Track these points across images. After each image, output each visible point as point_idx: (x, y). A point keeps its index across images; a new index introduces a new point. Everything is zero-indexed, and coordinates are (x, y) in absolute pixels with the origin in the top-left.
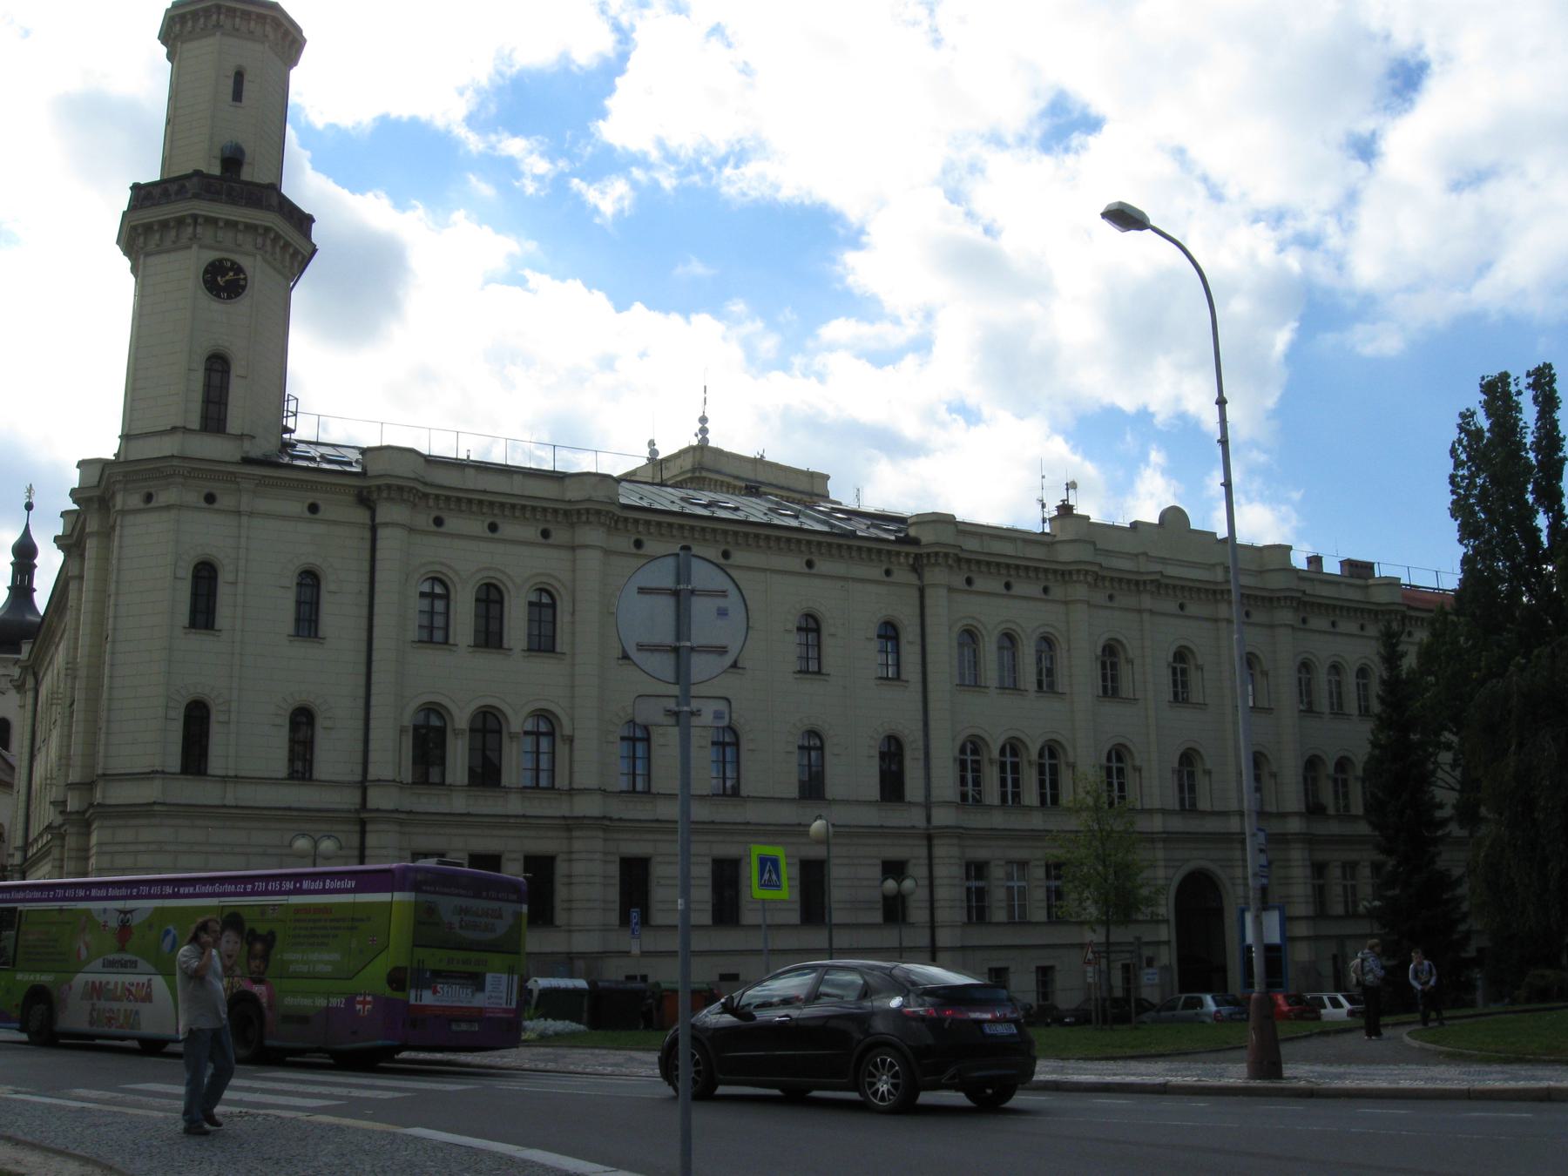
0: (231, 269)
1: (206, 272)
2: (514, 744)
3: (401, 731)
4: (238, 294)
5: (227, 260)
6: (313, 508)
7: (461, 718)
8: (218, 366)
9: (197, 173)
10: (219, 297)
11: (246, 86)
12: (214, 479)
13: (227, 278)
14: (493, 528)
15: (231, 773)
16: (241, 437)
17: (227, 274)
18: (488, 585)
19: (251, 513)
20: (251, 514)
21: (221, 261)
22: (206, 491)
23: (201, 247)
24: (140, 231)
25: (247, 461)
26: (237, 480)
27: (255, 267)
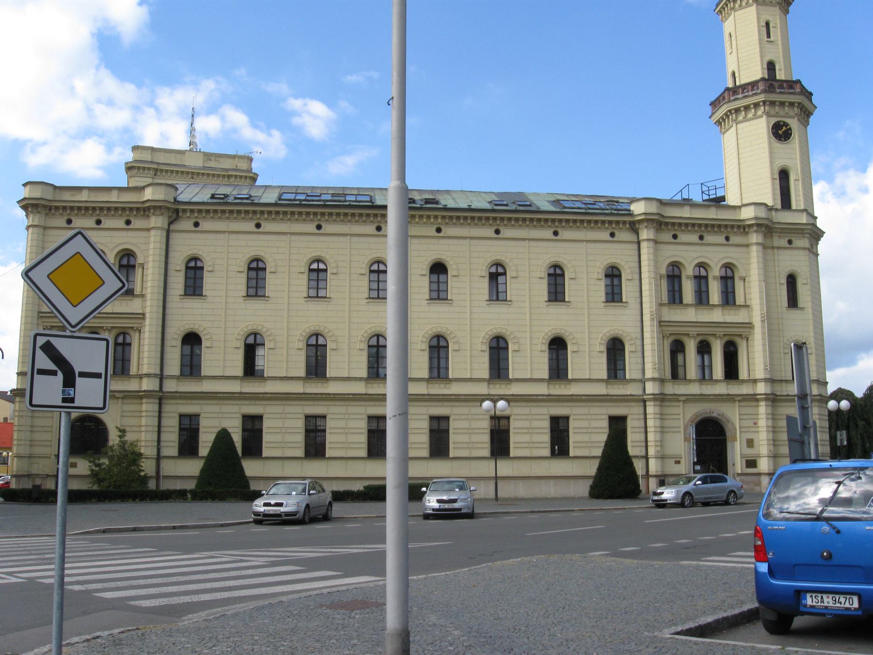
1: (773, 128)
8: (784, 175)
9: (763, 79)
11: (771, 29)
13: (783, 130)
21: (778, 122)
22: (788, 238)
24: (733, 111)
27: (794, 124)
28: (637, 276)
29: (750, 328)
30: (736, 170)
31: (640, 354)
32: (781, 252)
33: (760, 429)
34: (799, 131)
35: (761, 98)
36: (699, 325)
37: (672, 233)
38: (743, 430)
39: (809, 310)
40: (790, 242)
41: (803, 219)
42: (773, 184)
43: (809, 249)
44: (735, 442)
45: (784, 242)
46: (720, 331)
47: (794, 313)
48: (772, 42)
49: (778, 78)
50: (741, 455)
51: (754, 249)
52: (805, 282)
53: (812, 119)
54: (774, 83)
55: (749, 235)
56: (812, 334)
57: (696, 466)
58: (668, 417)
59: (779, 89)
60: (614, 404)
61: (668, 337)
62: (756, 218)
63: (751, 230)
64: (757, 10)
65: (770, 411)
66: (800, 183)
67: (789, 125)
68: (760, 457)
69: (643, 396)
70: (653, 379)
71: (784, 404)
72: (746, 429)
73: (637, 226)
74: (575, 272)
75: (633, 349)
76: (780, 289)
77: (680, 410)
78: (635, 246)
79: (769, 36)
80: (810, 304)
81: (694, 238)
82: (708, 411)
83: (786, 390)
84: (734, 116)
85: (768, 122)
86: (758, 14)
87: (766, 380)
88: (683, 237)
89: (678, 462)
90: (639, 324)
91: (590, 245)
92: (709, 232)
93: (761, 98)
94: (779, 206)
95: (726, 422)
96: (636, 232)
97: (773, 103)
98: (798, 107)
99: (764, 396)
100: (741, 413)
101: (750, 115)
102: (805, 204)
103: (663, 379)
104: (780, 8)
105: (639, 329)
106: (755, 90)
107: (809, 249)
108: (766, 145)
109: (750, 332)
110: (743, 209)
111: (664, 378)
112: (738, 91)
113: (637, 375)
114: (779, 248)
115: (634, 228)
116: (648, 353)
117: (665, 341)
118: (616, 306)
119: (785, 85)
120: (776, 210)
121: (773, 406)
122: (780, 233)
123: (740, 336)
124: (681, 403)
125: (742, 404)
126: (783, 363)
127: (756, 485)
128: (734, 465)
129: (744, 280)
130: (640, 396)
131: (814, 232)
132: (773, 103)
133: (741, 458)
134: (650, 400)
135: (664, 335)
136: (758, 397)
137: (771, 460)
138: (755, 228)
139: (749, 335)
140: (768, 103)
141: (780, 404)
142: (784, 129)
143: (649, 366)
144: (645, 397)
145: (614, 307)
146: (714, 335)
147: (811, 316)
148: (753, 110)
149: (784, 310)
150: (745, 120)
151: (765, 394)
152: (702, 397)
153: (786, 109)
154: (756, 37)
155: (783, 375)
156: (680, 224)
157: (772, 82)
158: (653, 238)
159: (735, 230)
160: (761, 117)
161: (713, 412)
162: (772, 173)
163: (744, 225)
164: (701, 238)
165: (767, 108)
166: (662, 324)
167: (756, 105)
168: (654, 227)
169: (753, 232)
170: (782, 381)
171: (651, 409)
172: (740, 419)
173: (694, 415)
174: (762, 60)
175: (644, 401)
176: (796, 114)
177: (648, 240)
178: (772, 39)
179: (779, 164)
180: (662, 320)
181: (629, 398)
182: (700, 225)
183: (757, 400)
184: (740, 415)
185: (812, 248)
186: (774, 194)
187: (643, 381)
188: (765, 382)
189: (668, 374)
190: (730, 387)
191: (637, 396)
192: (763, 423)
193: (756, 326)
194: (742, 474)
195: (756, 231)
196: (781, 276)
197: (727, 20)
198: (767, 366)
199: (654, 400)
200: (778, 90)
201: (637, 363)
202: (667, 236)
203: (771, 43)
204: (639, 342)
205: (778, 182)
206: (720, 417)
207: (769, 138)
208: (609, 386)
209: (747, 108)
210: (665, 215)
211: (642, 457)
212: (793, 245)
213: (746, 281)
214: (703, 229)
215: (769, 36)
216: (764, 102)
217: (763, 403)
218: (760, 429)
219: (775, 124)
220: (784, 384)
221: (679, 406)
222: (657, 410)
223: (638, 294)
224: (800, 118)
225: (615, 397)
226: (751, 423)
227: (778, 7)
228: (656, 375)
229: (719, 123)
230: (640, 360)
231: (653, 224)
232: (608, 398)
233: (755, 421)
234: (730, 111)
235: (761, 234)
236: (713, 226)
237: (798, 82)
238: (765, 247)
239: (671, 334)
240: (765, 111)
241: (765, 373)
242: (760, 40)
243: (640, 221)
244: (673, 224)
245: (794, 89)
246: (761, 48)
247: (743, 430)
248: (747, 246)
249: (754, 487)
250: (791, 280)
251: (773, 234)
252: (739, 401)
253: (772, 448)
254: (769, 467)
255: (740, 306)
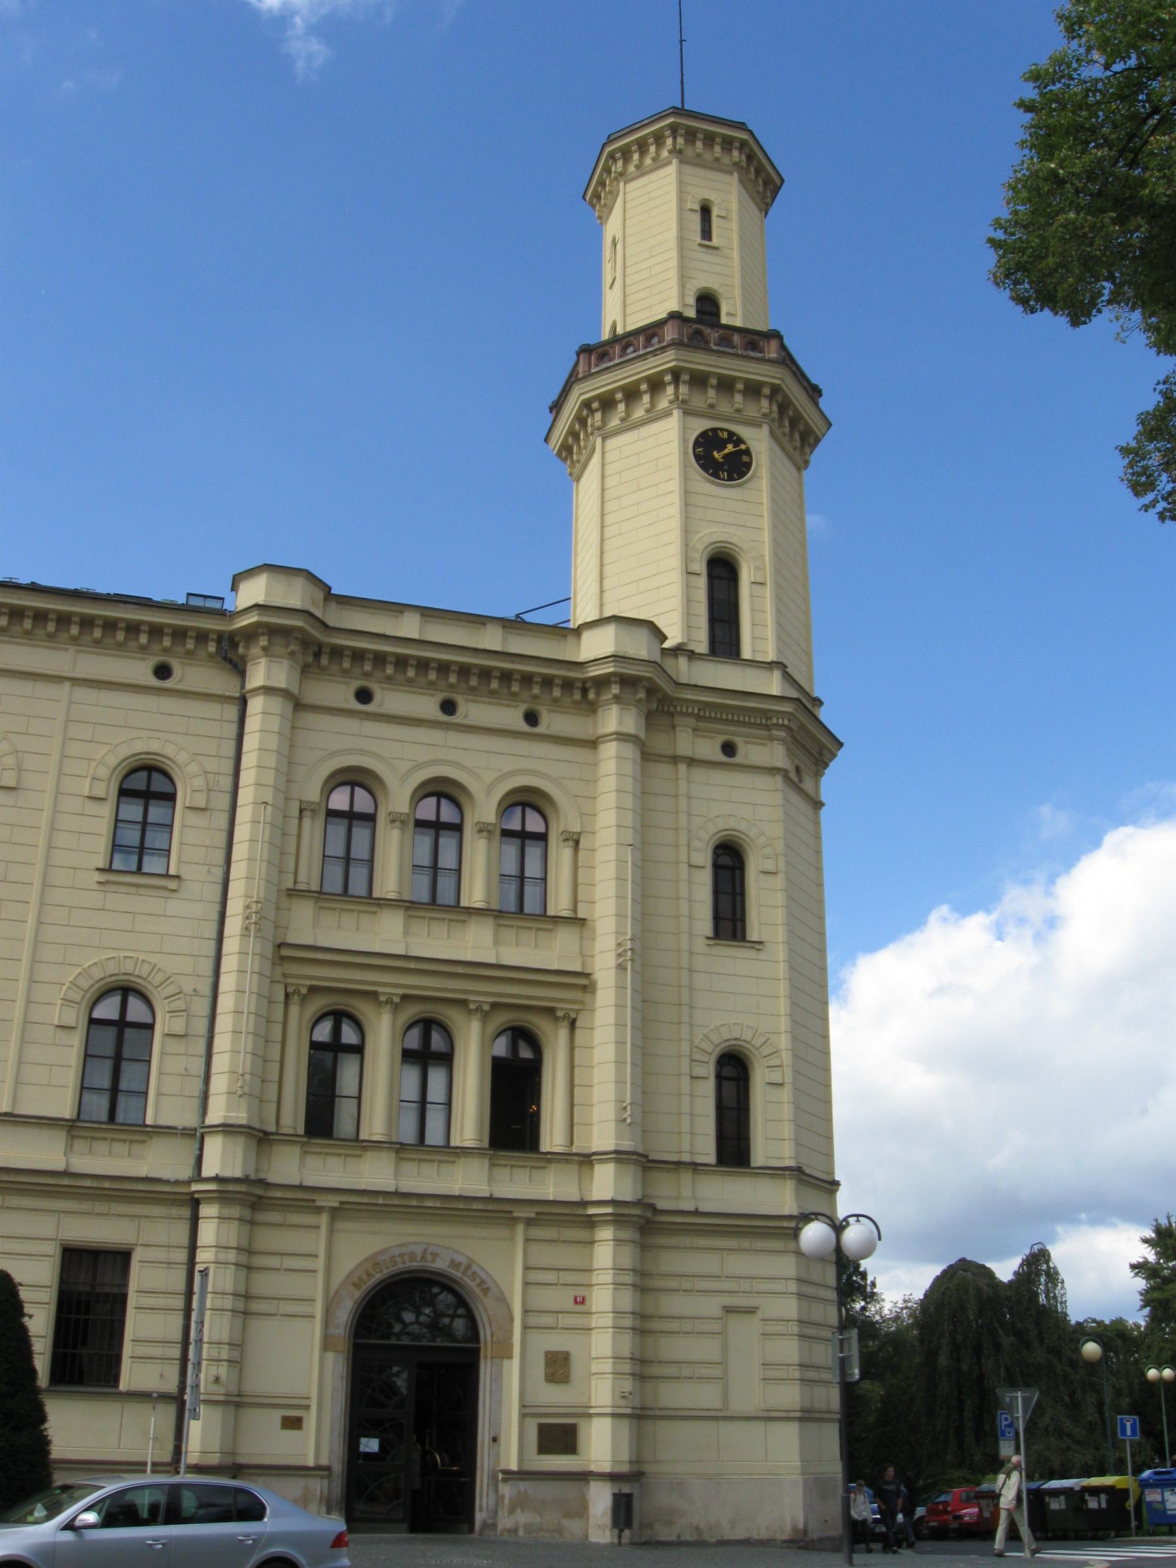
0: (729, 441)
1: (697, 444)
4: (742, 475)
5: (722, 430)
9: (675, 316)
10: (718, 477)
11: (715, 221)
13: (726, 451)
17: (726, 448)
21: (714, 430)
24: (595, 405)
28: (224, 801)
29: (584, 988)
30: (595, 562)
31: (201, 1048)
32: (699, 774)
33: (595, 1321)
34: (772, 462)
35: (666, 361)
36: (412, 965)
37: (356, 684)
38: (534, 1320)
39: (779, 952)
40: (729, 749)
41: (774, 685)
42: (688, 588)
43: (784, 772)
44: (506, 1362)
45: (710, 749)
46: (482, 992)
47: (730, 957)
48: (716, 248)
49: (724, 320)
50: (523, 1406)
51: (609, 750)
52: (769, 865)
53: (817, 457)
54: (707, 331)
55: (600, 711)
56: (784, 1024)
57: (363, 1440)
58: (273, 1262)
59: (718, 345)
60: (86, 1206)
61: (304, 999)
62: (616, 657)
63: (606, 696)
64: (680, 173)
65: (627, 1262)
66: (768, 591)
67: (743, 442)
68: (590, 1416)
69: (189, 1182)
70: (227, 1129)
71: (687, 1241)
72: (547, 1320)
73: (241, 650)
74: (20, 769)
75: (178, 1026)
76: (690, 882)
77: (318, 1242)
78: (232, 712)
79: (707, 233)
80: (780, 934)
81: (427, 705)
82: (418, 1250)
83: (694, 1197)
84: (598, 416)
85: (684, 429)
86: (681, 182)
87: (619, 1156)
88: (388, 700)
89: (293, 1424)
90: (210, 948)
91: (81, 693)
92: (472, 690)
93: (666, 361)
94: (702, 647)
95: (477, 1290)
96: (239, 669)
97: (699, 380)
98: (771, 398)
99: (609, 1210)
100: (532, 1262)
101: (639, 413)
102: (779, 651)
103: (266, 1133)
104: (741, 181)
105: (207, 967)
106: (652, 345)
107: (784, 772)
108: (675, 485)
109: (582, 1002)
110: (587, 636)
111: (272, 1129)
112: (611, 351)
113: (186, 1118)
114: (692, 762)
115: (234, 657)
116: (222, 1042)
117: (294, 1010)
118: (138, 886)
119: (736, 338)
120: (692, 655)
121: (643, 1247)
122: (698, 718)
123: (550, 1012)
124: (324, 1219)
125: (537, 1232)
126: (686, 1108)
127: (569, 1515)
128: (495, 1440)
129: (577, 842)
130: (177, 1183)
131: (802, 727)
132: (699, 380)
133: (523, 1416)
134: (211, 1197)
135: (290, 990)
136: (592, 1211)
137: (625, 1427)
138: (615, 689)
139: (578, 1011)
140: (685, 377)
141: (673, 1241)
142: (730, 448)
143: (219, 1084)
144: (195, 1187)
145: (133, 890)
146: (464, 1003)
147: (782, 970)
148: (646, 398)
149: (700, 944)
150: (628, 426)
151: (613, 1202)
152: (395, 1201)
153: (738, 398)
154: (672, 234)
155: (686, 1146)
156: (380, 659)
157: (702, 327)
158: (283, 685)
159: (557, 692)
160: (667, 414)
161: (435, 1255)
162: (687, 559)
163: (584, 681)
164: (448, 707)
165: (684, 389)
166: (285, 952)
167: (655, 385)
168: (292, 654)
169: (608, 702)
170: (679, 1163)
171: (208, 1232)
172: (526, 1284)
173: (366, 1261)
174: (682, 286)
175: (195, 1203)
176: (764, 415)
177: (267, 690)
178: (715, 241)
179: (710, 534)
180: (291, 939)
181: (140, 1187)
182: (444, 668)
183: (591, 1223)
184: (527, 1268)
185: (801, 781)
186: (688, 614)
187: (197, 1135)
188: (618, 1161)
189: (293, 1116)
190: (502, 1173)
191: (167, 1182)
192: (602, 1299)
193: (601, 983)
194: (523, 1475)
195: (617, 699)
196: (696, 844)
197: (610, 213)
198: (625, 1108)
199: (223, 1197)
200: (716, 348)
201: (187, 1074)
202: (341, 693)
203: (710, 251)
204: (201, 1007)
205: (702, 582)
206: (458, 1274)
207: (685, 466)
208: (79, 1145)
209: (631, 394)
210: (331, 623)
211: (164, 1397)
212: (738, 759)
213: (581, 845)
214: (453, 679)
215: (707, 233)
216: (676, 374)
217: (606, 1234)
218: (595, 1321)
219: (703, 435)
220: (686, 1177)
221: (318, 1227)
222: (232, 1234)
223: (219, 856)
224: (778, 433)
225: (88, 1183)
226: (562, 1299)
227: (736, 175)
228: (241, 1116)
229: (566, 451)
230: (198, 1066)
231: (287, 646)
232: (66, 1182)
233: (580, 1292)
234: (587, 404)
235: (634, 710)
236: (485, 674)
237: (775, 335)
238: (647, 756)
239: (313, 990)
240: (678, 398)
241: (619, 1136)
242: (681, 240)
243: (250, 634)
244: (358, 656)
245: (764, 353)
246: (682, 257)
247: (534, 1320)
248: (593, 744)
249: (566, 1523)
250: (726, 860)
251: (678, 720)
252: (529, 1222)
253: (627, 1385)
254: (615, 1449)
255: (557, 919)
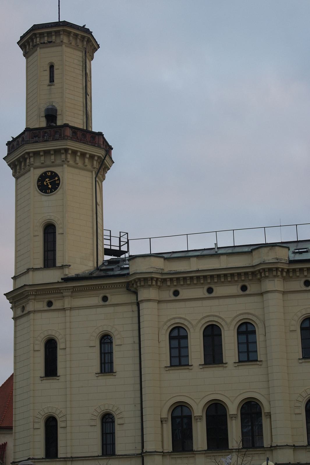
2: (234, 421)
3: (162, 421)
5: (48, 171)
6: (105, 299)
7: (233, 408)
12: (75, 291)
14: (210, 290)
15: (69, 456)
16: (63, 267)
18: (212, 326)
19: (71, 308)
20: (71, 309)
21: (45, 173)
23: (35, 168)
25: (66, 280)
26: (61, 291)
32: (38, 315)
122: (35, 295)
219: (41, 176)
